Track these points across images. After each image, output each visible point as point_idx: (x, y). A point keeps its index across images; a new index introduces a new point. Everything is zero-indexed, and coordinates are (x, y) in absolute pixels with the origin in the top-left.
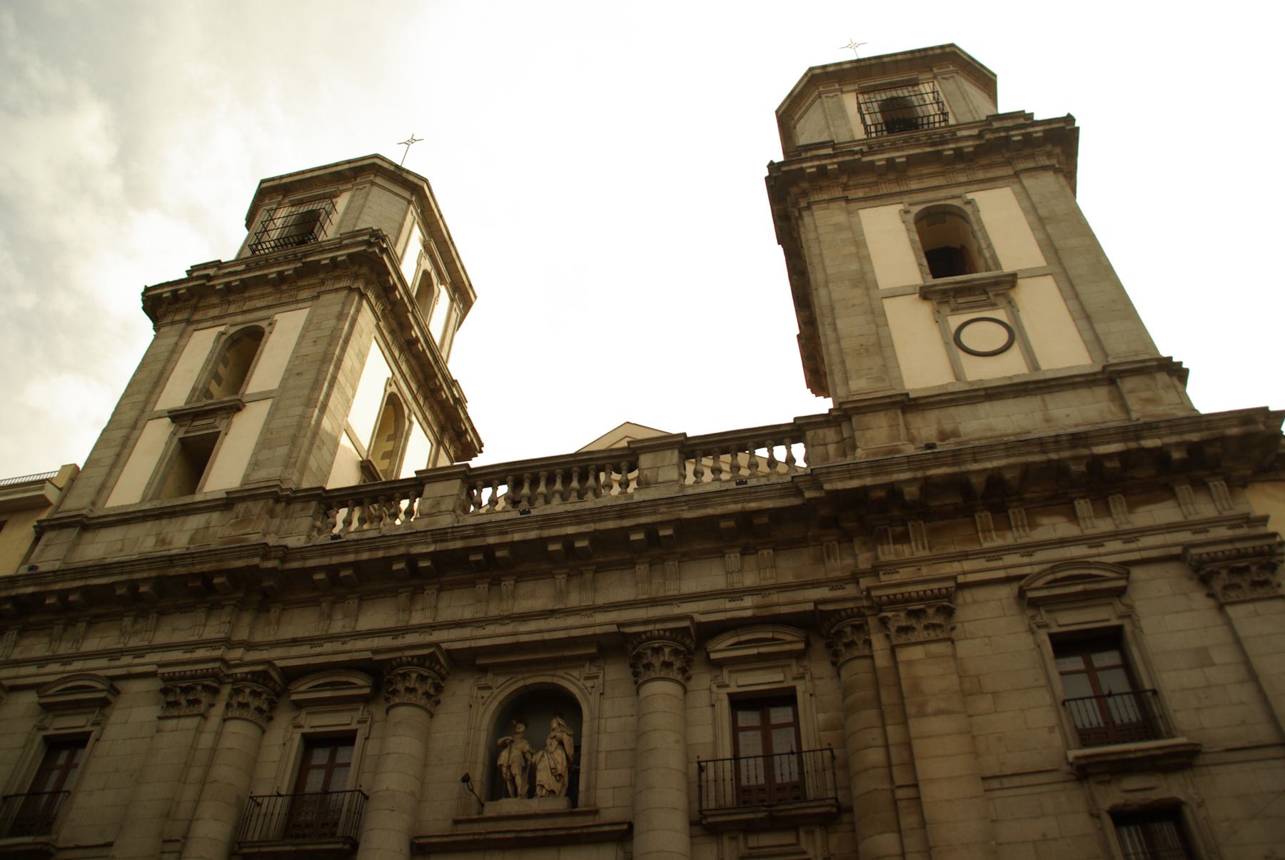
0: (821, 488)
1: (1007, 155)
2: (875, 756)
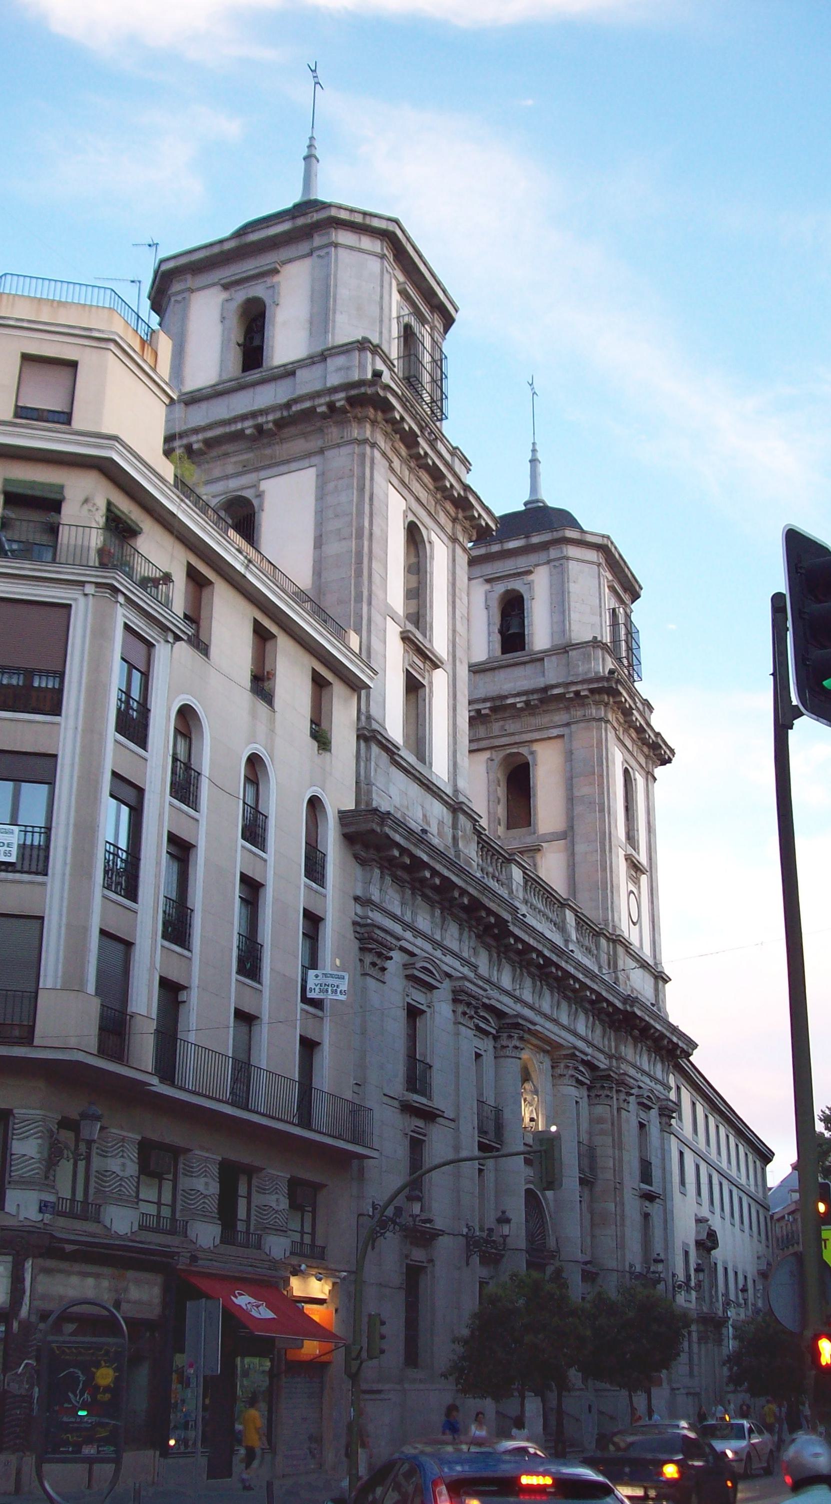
0: (632, 1006)
1: (651, 754)
2: (611, 1164)
